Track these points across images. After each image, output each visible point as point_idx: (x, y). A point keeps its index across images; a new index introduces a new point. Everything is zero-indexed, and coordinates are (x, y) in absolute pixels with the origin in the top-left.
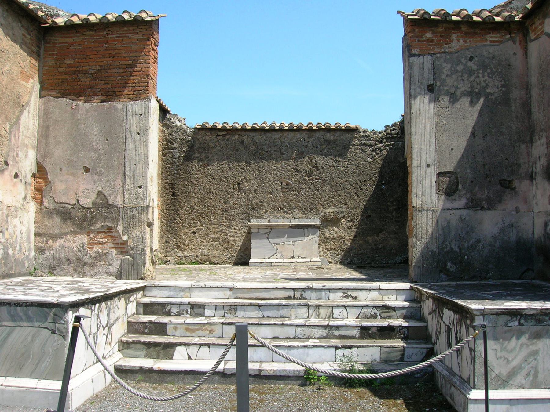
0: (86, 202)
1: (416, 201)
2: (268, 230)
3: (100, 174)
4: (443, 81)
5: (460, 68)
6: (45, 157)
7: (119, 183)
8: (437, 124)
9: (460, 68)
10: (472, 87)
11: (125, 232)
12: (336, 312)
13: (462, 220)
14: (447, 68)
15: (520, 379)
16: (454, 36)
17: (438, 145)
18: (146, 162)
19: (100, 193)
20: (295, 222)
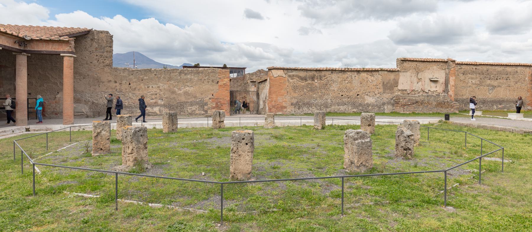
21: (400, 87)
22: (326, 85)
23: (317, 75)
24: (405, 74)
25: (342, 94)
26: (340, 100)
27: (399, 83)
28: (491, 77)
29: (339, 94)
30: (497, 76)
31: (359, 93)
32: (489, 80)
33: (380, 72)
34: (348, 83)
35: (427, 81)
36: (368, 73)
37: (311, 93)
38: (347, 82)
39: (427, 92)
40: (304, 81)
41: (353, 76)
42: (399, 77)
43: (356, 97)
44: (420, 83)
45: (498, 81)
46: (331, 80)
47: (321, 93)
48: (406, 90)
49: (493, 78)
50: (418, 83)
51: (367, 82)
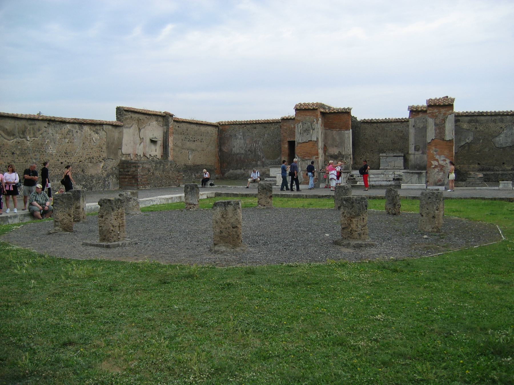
0: (336, 154)
1: (410, 152)
2: (386, 157)
3: (339, 147)
4: (417, 124)
5: (421, 121)
6: (326, 143)
7: (343, 149)
8: (415, 135)
9: (421, 121)
10: (424, 126)
11: (345, 160)
12: (390, 176)
13: (420, 156)
14: (418, 121)
15: (409, 182)
16: (420, 113)
17: (415, 139)
18: (350, 144)
19: (339, 152)
20: (394, 155)
21: (125, 150)
22: (42, 145)
23: (28, 128)
24: (128, 130)
25: (61, 161)
26: (60, 170)
27: (123, 144)
28: (190, 138)
29: (58, 160)
30: (194, 137)
31: (81, 159)
32: (188, 143)
33: (104, 126)
34: (68, 142)
35: (148, 141)
36: (91, 127)
37: (21, 159)
38: (67, 140)
39: (148, 156)
40: (12, 138)
41: (75, 131)
42: (123, 134)
43: (78, 165)
44: (142, 145)
45: (196, 143)
46: (48, 138)
47: (36, 159)
48: (129, 154)
49: (191, 139)
50: (140, 144)
51: (91, 141)
